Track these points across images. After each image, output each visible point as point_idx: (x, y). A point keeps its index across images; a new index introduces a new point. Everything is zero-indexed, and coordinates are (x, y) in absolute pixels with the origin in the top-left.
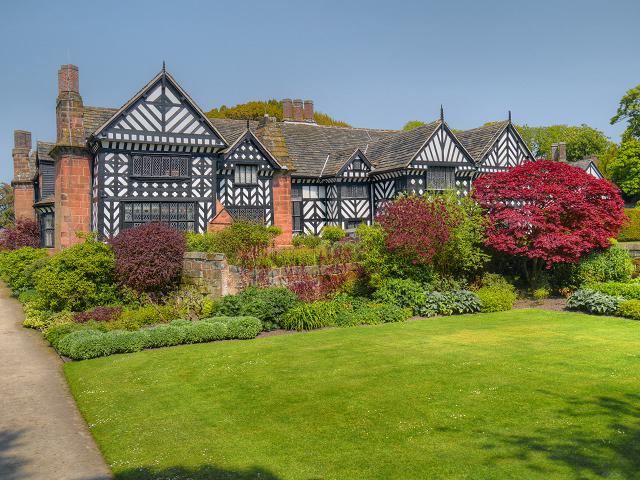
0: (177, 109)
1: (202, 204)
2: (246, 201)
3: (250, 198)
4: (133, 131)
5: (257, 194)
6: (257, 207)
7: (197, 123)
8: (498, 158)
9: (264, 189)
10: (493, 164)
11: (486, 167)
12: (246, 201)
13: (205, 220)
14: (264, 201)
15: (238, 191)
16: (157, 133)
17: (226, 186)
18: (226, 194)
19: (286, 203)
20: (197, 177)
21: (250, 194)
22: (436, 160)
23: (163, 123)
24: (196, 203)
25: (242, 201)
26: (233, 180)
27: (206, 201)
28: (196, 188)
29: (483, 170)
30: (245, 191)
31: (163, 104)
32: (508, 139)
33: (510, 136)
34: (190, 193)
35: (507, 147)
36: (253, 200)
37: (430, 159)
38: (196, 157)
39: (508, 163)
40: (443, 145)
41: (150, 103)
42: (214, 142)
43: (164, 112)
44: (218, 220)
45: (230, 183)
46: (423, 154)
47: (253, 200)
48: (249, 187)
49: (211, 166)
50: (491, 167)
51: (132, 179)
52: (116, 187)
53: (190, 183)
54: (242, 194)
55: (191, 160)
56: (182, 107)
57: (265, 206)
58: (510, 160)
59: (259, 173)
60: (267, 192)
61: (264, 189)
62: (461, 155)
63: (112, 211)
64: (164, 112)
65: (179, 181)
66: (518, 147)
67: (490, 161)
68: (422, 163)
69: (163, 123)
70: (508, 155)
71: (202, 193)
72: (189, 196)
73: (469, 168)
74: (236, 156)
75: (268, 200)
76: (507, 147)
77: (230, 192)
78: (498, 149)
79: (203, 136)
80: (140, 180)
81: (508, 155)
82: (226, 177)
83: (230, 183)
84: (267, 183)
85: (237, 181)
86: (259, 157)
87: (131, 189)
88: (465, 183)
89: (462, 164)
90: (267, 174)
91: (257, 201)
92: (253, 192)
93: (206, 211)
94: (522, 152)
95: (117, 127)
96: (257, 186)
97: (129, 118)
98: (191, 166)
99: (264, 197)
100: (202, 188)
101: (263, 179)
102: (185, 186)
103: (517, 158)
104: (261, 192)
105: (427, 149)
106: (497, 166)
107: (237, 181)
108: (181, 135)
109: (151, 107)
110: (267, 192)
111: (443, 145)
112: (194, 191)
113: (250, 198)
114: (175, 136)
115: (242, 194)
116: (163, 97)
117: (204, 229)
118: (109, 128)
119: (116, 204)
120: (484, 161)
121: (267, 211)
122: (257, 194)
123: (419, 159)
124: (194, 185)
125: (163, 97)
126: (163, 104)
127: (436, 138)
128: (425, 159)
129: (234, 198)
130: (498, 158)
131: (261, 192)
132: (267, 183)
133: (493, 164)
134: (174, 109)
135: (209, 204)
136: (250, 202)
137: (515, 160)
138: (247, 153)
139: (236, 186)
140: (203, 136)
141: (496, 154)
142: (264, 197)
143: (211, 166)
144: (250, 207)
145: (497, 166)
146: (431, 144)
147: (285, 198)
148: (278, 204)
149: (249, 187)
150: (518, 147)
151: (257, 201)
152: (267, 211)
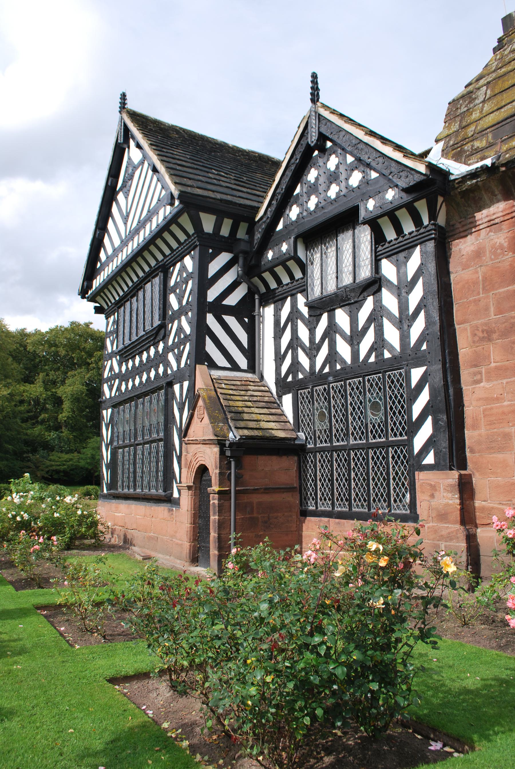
2: (344, 349)
3: (355, 338)
6: (383, 367)
9: (403, 289)
14: (404, 337)
18: (295, 343)
21: (354, 321)
25: (333, 356)
30: (342, 317)
34: (167, 364)
38: (174, 265)
57: (409, 357)
60: (415, 297)
75: (418, 327)
77: (303, 333)
90: (409, 227)
91: (380, 343)
95: (99, 265)
96: (375, 284)
99: (404, 322)
104: (389, 300)
107: (316, 292)
110: (415, 297)
129: (312, 351)
136: (355, 354)
139: (317, 308)
142: (404, 322)
144: (358, 369)
148: (488, 335)
149: (349, 298)
151: (380, 343)
152: (417, 374)
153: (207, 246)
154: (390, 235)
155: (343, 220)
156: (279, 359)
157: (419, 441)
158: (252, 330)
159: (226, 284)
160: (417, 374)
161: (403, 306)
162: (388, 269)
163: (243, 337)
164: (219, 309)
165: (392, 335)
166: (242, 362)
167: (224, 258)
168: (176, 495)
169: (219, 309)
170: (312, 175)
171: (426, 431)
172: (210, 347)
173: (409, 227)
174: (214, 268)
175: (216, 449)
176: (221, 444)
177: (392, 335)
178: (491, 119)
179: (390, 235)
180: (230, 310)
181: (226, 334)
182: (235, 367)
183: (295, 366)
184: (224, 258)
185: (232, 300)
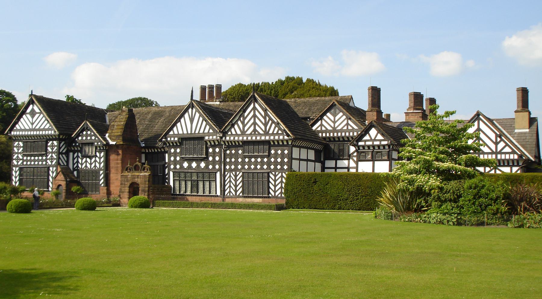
0: (38, 115)
1: (51, 168)
2: (88, 166)
3: (91, 164)
4: (21, 130)
5: (95, 161)
7: (46, 122)
8: (244, 126)
9: (100, 158)
10: (239, 132)
11: (232, 134)
12: (88, 166)
13: (52, 177)
15: (84, 160)
16: (30, 130)
17: (78, 157)
18: (78, 162)
19: (118, 167)
20: (50, 153)
22: (185, 132)
23: (32, 124)
24: (49, 168)
25: (86, 166)
26: (81, 153)
27: (53, 166)
28: (49, 159)
29: (228, 138)
30: (88, 160)
31: (33, 113)
32: (254, 109)
33: (257, 105)
35: (255, 116)
36: (93, 165)
37: (181, 132)
39: (255, 130)
40: (192, 120)
41: (28, 113)
42: (53, 132)
43: (33, 117)
44: (59, 177)
45: (80, 155)
46: (175, 129)
47: (93, 165)
48: (91, 158)
49: (14, 147)
50: (237, 135)
51: (24, 155)
52: (18, 159)
53: (47, 156)
54: (86, 161)
55: (47, 143)
56: (41, 113)
57: (100, 169)
58: (257, 128)
59: (96, 148)
61: (100, 158)
62: (208, 127)
63: (16, 172)
64: (33, 117)
65: (42, 155)
66: (266, 114)
67: (237, 129)
68: (174, 136)
69: (32, 124)
70: (255, 124)
71: (52, 162)
72: (46, 164)
73: (215, 137)
74: (80, 138)
75: (102, 165)
76: (255, 116)
77: (80, 160)
78: (245, 119)
79: (48, 129)
80: (27, 156)
81: (255, 124)
82: (78, 151)
83: (80, 155)
84: (102, 154)
85: (83, 153)
86: (93, 138)
87: (24, 161)
88: (217, 150)
89: (209, 134)
91: (95, 166)
92: (93, 160)
93: (53, 172)
94: (270, 119)
97: (20, 123)
98: (47, 146)
99: (100, 163)
100: (52, 159)
101: (100, 153)
102: (44, 158)
103: (265, 125)
104: (97, 159)
105: (179, 125)
106: (243, 133)
108: (39, 130)
109: (28, 116)
110: (102, 160)
111: (192, 120)
112: (48, 161)
113: (91, 164)
114: (37, 130)
115: (86, 161)
116: (33, 110)
117: (52, 183)
118: (11, 129)
119: (17, 168)
120: (230, 130)
121: (101, 172)
122: (95, 161)
123: (171, 133)
124: (48, 158)
125: (33, 110)
126: (33, 113)
127: (186, 115)
128: (176, 132)
130: (244, 126)
131: (97, 159)
132: (102, 154)
133: (239, 132)
134: (37, 115)
135: (55, 168)
137: (263, 128)
138: (87, 135)
140: (48, 129)
141: (243, 123)
143: (14, 147)
145: (243, 133)
146: (182, 120)
147: (118, 164)
150: (266, 114)
151: (95, 166)
153: (60, 140)
154: (98, 149)
155: (91, 144)
156: (74, 164)
157: (101, 182)
158: (68, 157)
159: (63, 149)
160: (101, 172)
161: (100, 161)
162: (98, 154)
163: (66, 159)
164: (62, 153)
165: (98, 165)
166: (65, 164)
167: (63, 143)
168: (50, 189)
169: (62, 153)
170: (84, 133)
171: (102, 181)
172: (60, 161)
173: (102, 148)
174: (61, 145)
175: (65, 182)
176: (66, 181)
177: (98, 165)
178: (116, 134)
179: (98, 149)
180: (64, 153)
181: (63, 157)
182: (64, 165)
183: (78, 166)
184: (63, 143)
185: (64, 152)
